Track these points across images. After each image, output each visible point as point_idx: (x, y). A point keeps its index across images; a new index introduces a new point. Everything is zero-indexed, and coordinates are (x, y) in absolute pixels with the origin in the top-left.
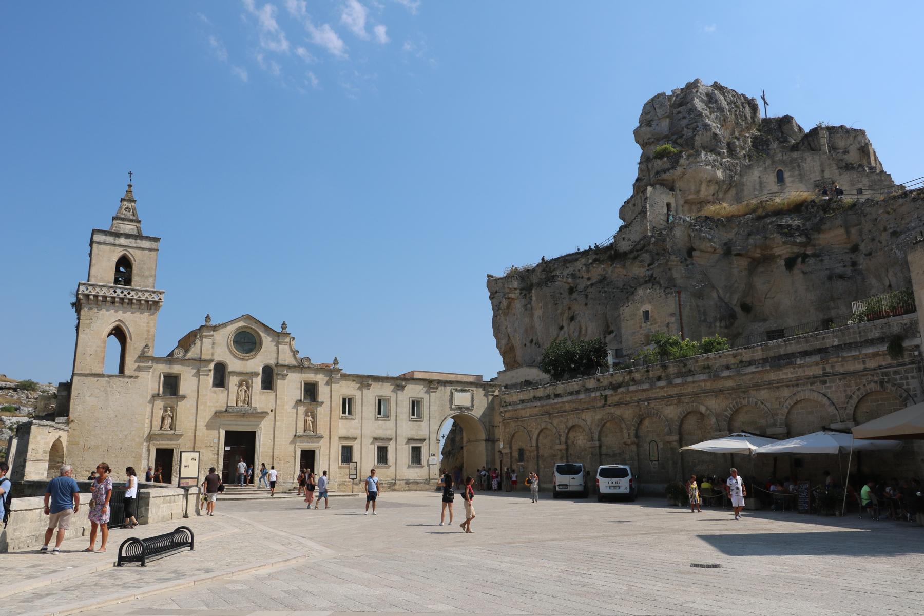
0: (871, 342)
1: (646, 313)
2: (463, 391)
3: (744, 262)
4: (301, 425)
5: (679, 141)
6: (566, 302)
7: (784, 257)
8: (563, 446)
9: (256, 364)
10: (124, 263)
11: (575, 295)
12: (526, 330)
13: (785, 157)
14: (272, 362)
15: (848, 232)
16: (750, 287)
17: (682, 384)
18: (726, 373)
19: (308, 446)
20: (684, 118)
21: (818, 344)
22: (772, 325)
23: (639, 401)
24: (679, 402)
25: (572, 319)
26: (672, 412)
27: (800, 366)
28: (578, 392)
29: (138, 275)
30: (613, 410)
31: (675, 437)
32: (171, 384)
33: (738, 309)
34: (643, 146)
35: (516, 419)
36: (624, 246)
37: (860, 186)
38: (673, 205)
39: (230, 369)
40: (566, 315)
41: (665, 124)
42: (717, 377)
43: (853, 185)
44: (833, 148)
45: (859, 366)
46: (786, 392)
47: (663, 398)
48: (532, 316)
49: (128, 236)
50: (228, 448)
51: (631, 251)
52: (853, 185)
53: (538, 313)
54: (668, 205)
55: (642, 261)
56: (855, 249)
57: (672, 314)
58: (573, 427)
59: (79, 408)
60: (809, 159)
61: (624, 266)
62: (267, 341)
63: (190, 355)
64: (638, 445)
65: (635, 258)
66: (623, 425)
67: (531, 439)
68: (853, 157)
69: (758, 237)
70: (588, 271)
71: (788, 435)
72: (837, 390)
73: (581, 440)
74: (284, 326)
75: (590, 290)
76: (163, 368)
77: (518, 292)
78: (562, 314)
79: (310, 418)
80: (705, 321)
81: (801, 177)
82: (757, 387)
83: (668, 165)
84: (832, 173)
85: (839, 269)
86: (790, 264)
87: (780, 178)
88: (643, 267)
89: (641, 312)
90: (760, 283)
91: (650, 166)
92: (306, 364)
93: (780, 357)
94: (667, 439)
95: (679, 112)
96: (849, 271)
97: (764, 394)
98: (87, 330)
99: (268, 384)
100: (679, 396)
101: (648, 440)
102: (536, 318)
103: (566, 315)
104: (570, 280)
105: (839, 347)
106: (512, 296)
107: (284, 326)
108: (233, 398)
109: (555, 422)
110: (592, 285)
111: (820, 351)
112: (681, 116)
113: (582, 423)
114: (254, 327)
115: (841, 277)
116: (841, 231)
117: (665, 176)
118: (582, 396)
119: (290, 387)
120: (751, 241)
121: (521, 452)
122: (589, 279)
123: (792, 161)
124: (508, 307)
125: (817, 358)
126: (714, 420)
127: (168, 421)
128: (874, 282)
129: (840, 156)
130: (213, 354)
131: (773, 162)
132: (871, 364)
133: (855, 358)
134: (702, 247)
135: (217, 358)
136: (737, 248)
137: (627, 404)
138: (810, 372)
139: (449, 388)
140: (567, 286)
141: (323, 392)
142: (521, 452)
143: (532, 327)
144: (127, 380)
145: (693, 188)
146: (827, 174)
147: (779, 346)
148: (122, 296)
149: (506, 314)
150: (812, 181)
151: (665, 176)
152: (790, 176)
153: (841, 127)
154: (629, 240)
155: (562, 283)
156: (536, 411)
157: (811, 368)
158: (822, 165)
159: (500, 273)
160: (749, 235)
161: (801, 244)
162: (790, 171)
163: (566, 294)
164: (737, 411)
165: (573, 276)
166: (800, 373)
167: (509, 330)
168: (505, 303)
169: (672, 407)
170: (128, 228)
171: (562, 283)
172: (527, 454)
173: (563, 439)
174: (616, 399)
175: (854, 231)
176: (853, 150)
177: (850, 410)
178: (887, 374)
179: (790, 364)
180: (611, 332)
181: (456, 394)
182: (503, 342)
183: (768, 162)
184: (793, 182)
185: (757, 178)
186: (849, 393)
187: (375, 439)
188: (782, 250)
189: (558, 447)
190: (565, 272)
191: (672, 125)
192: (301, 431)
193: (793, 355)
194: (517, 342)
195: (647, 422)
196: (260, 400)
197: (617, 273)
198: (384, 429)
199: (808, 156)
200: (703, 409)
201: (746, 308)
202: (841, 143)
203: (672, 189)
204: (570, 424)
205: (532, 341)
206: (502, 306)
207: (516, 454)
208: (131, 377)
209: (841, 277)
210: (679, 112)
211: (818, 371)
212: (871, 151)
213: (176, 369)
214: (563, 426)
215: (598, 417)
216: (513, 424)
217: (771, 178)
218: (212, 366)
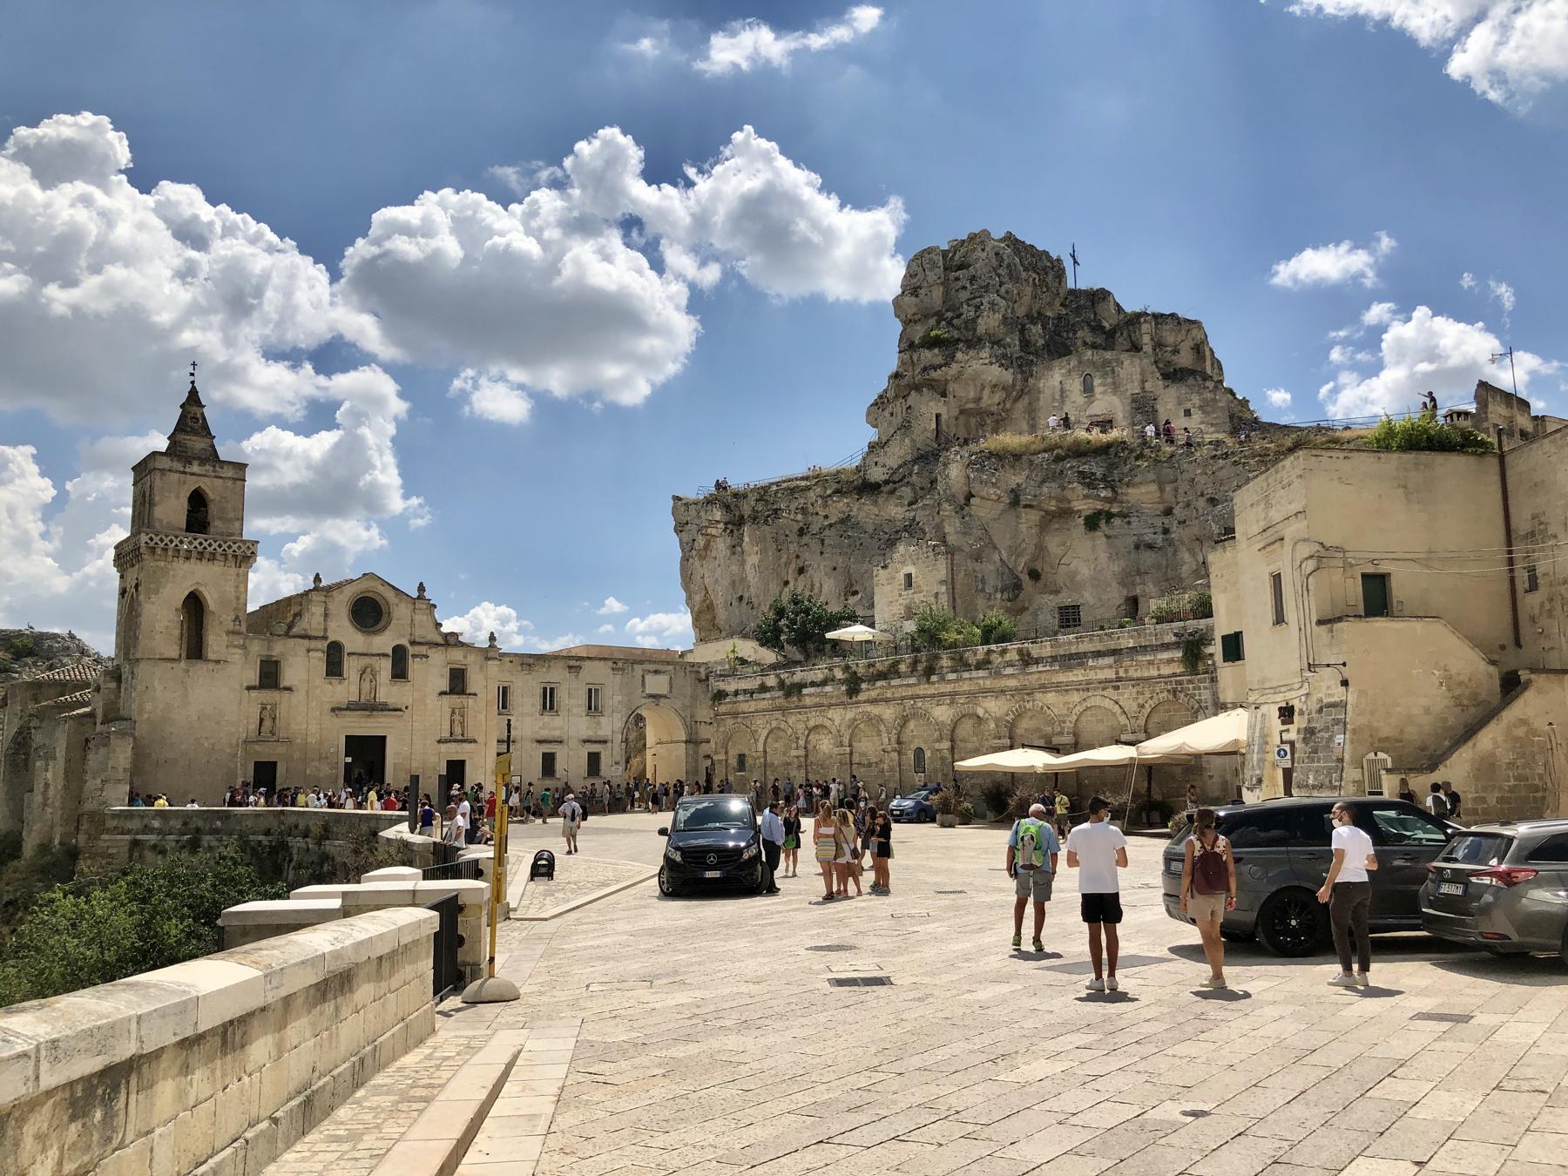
0: (1166, 647)
1: (909, 576)
2: (656, 672)
3: (1034, 516)
4: (447, 726)
5: (955, 321)
6: (793, 547)
7: (1084, 514)
8: (802, 752)
9: (385, 642)
10: (198, 500)
11: (805, 539)
12: (734, 582)
14: (405, 642)
15: (1162, 490)
16: (1041, 548)
17: (957, 681)
18: (1009, 671)
19: (454, 752)
20: (964, 288)
21: (1112, 645)
22: (1067, 599)
23: (902, 699)
24: (952, 702)
25: (801, 571)
26: (943, 713)
27: (1092, 668)
28: (824, 683)
29: (220, 519)
30: (869, 708)
31: (946, 745)
32: (270, 676)
33: (1025, 577)
34: (907, 323)
35: (735, 715)
36: (877, 474)
37: (1188, 405)
38: (944, 417)
39: (348, 648)
40: (793, 565)
41: (938, 293)
42: (998, 674)
43: (1180, 404)
44: (1158, 345)
45: (1154, 673)
46: (1075, 697)
47: (933, 696)
48: (743, 563)
49: (203, 462)
50: (349, 760)
51: (887, 482)
53: (753, 559)
54: (938, 416)
55: (901, 497)
56: (1168, 512)
57: (941, 582)
58: (816, 727)
59: (148, 706)
61: (875, 503)
62: (401, 612)
63: (295, 630)
64: (899, 753)
65: (892, 492)
66: (882, 727)
67: (756, 741)
68: (1185, 359)
69: (1053, 485)
70: (825, 505)
71: (1076, 747)
72: (1127, 697)
73: (825, 745)
74: (421, 588)
75: (827, 532)
76: (257, 648)
77: (721, 525)
78: (787, 564)
79: (457, 717)
80: (983, 590)
81: (1116, 387)
82: (1043, 688)
83: (939, 360)
84: (1155, 385)
85: (1149, 538)
86: (1092, 523)
87: (1088, 389)
88: (902, 505)
89: (901, 576)
90: (1053, 544)
91: (915, 358)
92: (452, 640)
93: (1071, 656)
94: (937, 746)
95: (957, 279)
96: (1159, 539)
97: (1051, 697)
98: (154, 598)
99: (400, 673)
100: (953, 694)
101: (913, 747)
102: (748, 567)
103: (793, 565)
104: (799, 517)
105: (1133, 650)
106: (714, 532)
107: (421, 588)
108: (354, 689)
109: (791, 720)
110: (831, 525)
111: (1114, 652)
112: (960, 284)
113: (828, 723)
114: (381, 589)
115: (1150, 547)
116: (1153, 487)
117: (935, 375)
118: (828, 689)
119: (430, 673)
120: (1045, 490)
121: (742, 759)
122: (826, 517)
123: (1106, 363)
124: (707, 547)
125: (1109, 660)
126: (993, 725)
127: (267, 723)
128: (1187, 556)
129: (1168, 356)
130: (326, 630)
132: (1166, 670)
133: (1150, 663)
134: (983, 493)
135: (332, 637)
136: (1025, 499)
137: (887, 701)
138: (1102, 675)
139: (638, 669)
140: (796, 527)
141: (475, 681)
142: (742, 759)
143: (743, 579)
144: (211, 666)
145: (972, 395)
146: (1148, 386)
147: (1070, 643)
148: (200, 548)
149: (702, 558)
151: (935, 375)
153: (1173, 315)
155: (789, 519)
156: (763, 705)
157: (1103, 670)
158: (1142, 373)
159: (691, 493)
160: (1043, 482)
161: (1106, 499)
163: (793, 537)
164: (1019, 716)
165: (804, 511)
166: (1092, 675)
167: (707, 581)
168: (701, 541)
169: (944, 708)
170: (197, 444)
171: (789, 519)
172: (749, 762)
173: (801, 743)
174: (873, 694)
175: (1168, 488)
176: (1186, 348)
177: (1142, 722)
178: (1180, 683)
179: (1081, 665)
180: (855, 593)
181: (648, 678)
182: (698, 598)
183: (1074, 363)
184: (1104, 393)
185: (1057, 384)
186: (1141, 701)
187: (539, 742)
188: (1084, 506)
189: (794, 753)
190: (793, 506)
191: (946, 294)
192: (446, 735)
193: (1085, 655)
194: (720, 597)
195: (912, 725)
196: (388, 692)
197: (866, 511)
198: (552, 726)
199: (1126, 358)
200: (980, 712)
201: (1035, 575)
202: (1170, 338)
203: (944, 395)
204: (812, 723)
205: (741, 598)
206: (696, 545)
207: (733, 762)
208: (218, 662)
209: (1150, 547)
210: (957, 279)
211: (1110, 674)
212: (1208, 353)
213: (278, 648)
214: (801, 726)
215: (850, 715)
216: (730, 722)
217: (1075, 385)
218: (324, 645)
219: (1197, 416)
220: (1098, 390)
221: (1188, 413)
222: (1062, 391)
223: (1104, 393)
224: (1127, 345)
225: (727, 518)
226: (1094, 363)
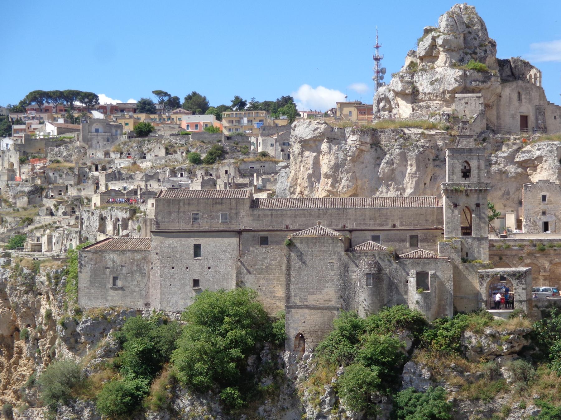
1: (544, 198)
5: (473, 55)
6: (431, 166)
13: (523, 85)
37: (555, 114)
43: (553, 113)
52: (553, 113)
60: (534, 90)
81: (530, 101)
87: (520, 99)
89: (541, 196)
123: (527, 88)
131: (517, 86)
150: (535, 104)
152: (525, 98)
154: (474, 131)
162: (525, 94)
184: (526, 102)
185: (508, 94)
191: (465, 38)
217: (515, 96)
219: (558, 119)
220: (524, 100)
221: (555, 118)
222: (510, 98)
223: (526, 102)
224: (509, 73)
225: (371, 142)
226: (522, 87)
